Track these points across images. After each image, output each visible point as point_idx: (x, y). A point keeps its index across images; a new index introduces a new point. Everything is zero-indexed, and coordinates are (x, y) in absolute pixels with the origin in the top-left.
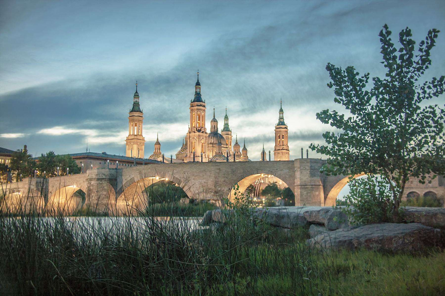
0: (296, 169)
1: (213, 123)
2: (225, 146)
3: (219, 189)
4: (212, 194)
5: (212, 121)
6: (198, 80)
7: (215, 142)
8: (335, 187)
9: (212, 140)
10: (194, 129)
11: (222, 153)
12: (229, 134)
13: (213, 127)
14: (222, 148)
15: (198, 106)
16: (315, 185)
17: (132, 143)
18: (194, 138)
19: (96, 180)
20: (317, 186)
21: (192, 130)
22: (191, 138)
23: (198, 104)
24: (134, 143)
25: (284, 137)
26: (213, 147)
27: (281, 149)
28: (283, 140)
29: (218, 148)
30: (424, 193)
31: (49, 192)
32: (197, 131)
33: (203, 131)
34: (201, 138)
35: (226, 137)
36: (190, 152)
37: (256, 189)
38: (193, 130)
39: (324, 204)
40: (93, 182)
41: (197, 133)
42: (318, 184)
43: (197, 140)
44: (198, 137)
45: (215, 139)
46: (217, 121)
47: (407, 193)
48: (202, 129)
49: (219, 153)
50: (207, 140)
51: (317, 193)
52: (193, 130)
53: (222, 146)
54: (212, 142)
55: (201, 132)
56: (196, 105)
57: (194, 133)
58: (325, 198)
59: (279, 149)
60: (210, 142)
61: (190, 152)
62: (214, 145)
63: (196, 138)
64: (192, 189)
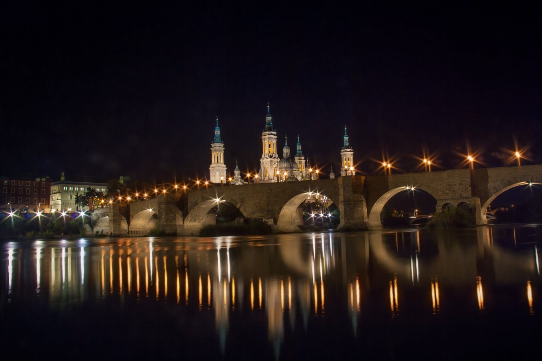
0: (339, 187)
2: (297, 169)
3: (271, 208)
4: (265, 213)
7: (288, 167)
8: (378, 202)
9: (285, 164)
10: (266, 155)
11: (293, 176)
14: (294, 171)
15: (269, 135)
16: (358, 201)
17: (215, 171)
18: (266, 163)
19: (164, 204)
20: (360, 202)
21: (265, 156)
22: (264, 164)
23: (269, 134)
24: (217, 170)
25: (350, 159)
28: (349, 162)
30: (457, 204)
31: (131, 216)
32: (269, 157)
33: (275, 156)
34: (273, 163)
35: (299, 161)
36: (264, 176)
37: (324, 206)
38: (266, 157)
39: (367, 219)
40: (162, 206)
41: (269, 159)
42: (360, 199)
43: (270, 165)
44: (270, 162)
45: (287, 164)
47: (442, 205)
48: (273, 155)
50: (278, 165)
51: (360, 208)
52: (266, 157)
53: (294, 169)
54: (285, 166)
55: (273, 158)
56: (267, 134)
57: (266, 159)
58: (369, 212)
60: (283, 167)
61: (264, 176)
62: (287, 169)
63: (268, 163)
64: (247, 209)
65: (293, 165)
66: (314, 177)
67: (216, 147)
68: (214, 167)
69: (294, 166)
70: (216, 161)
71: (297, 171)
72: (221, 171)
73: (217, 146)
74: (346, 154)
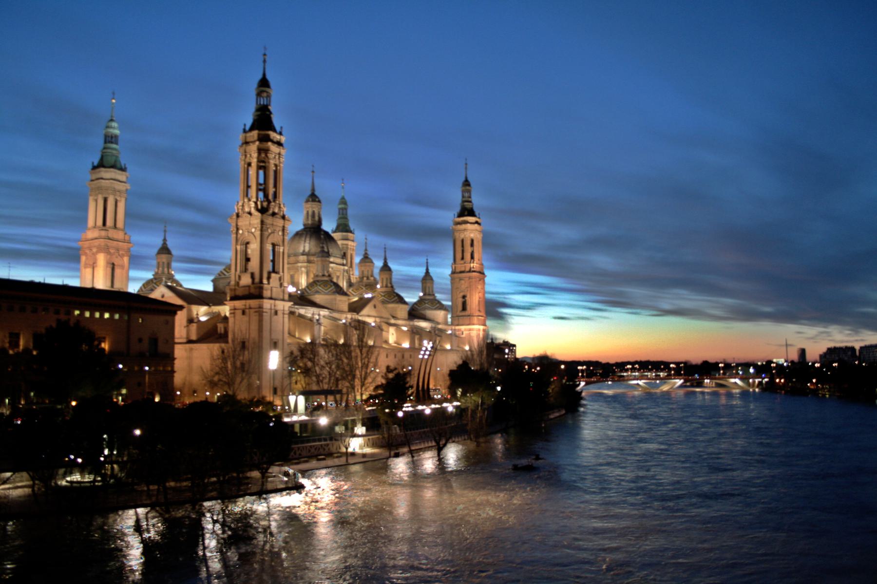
1: (310, 204)
2: (339, 261)
5: (307, 201)
6: (264, 75)
7: (314, 250)
11: (329, 276)
12: (349, 238)
13: (310, 213)
14: (332, 265)
17: (94, 250)
22: (241, 232)
24: (100, 250)
26: (309, 262)
27: (468, 269)
29: (320, 263)
32: (257, 210)
38: (247, 210)
45: (313, 242)
46: (319, 201)
49: (323, 275)
53: (332, 259)
54: (307, 249)
59: (463, 269)
62: (312, 258)
65: (329, 247)
66: (384, 285)
67: (102, 179)
68: (92, 240)
69: (331, 251)
70: (100, 222)
71: (340, 265)
72: (112, 251)
73: (104, 177)
74: (465, 230)
